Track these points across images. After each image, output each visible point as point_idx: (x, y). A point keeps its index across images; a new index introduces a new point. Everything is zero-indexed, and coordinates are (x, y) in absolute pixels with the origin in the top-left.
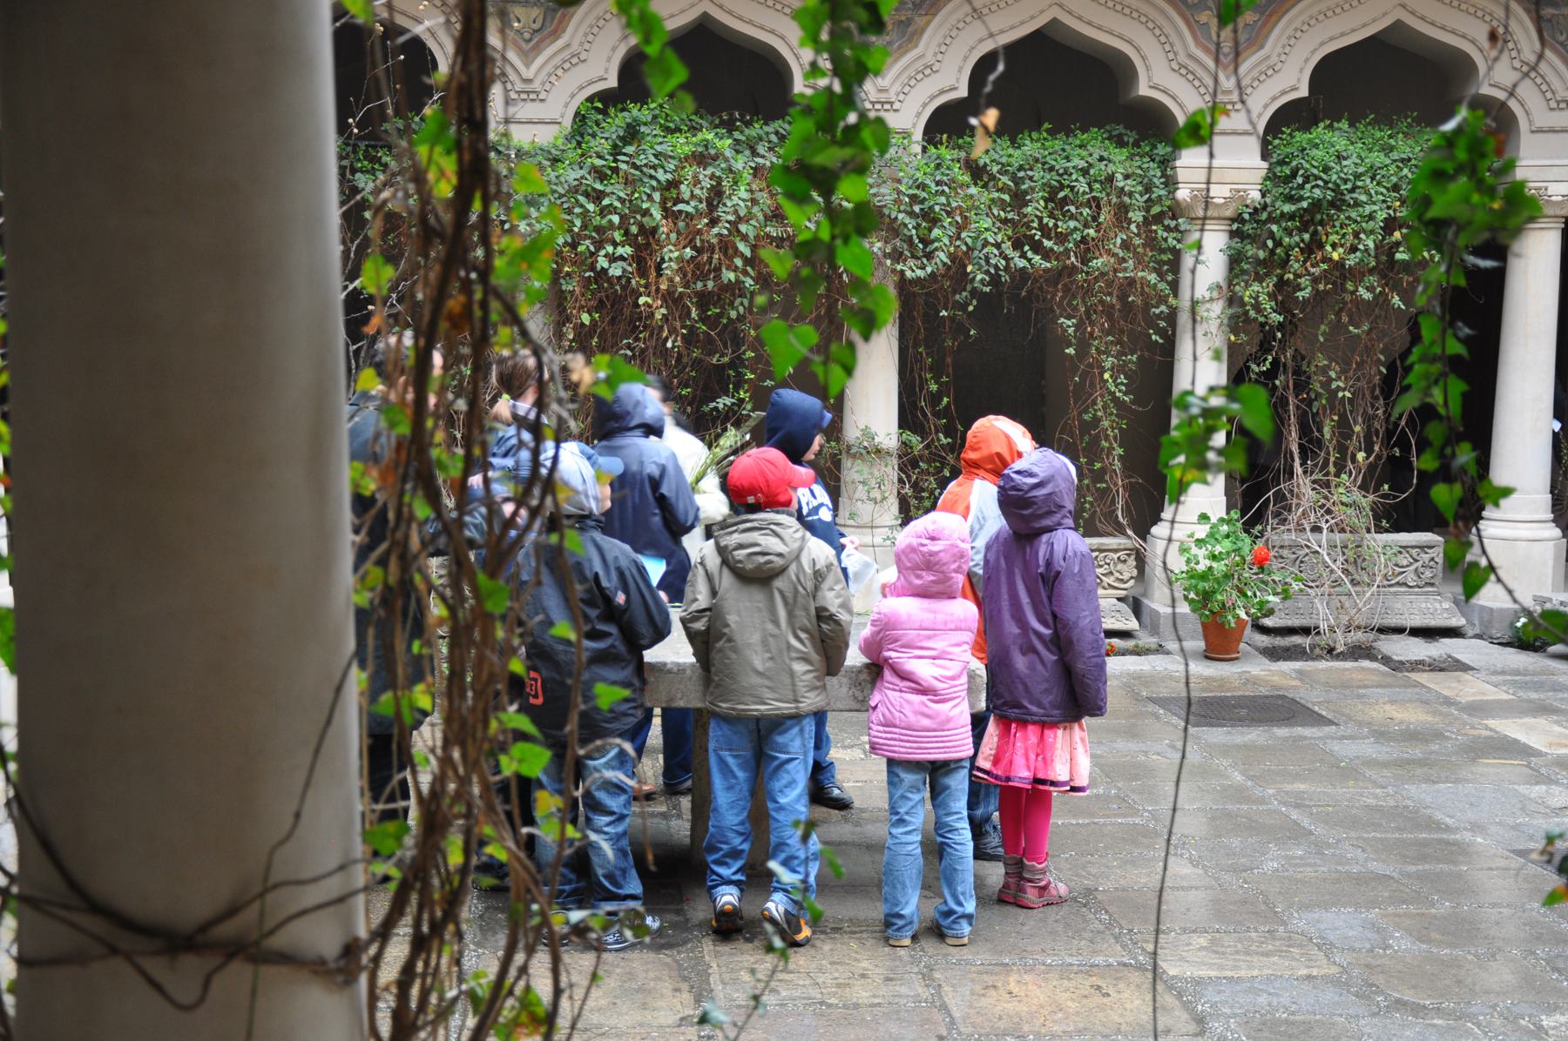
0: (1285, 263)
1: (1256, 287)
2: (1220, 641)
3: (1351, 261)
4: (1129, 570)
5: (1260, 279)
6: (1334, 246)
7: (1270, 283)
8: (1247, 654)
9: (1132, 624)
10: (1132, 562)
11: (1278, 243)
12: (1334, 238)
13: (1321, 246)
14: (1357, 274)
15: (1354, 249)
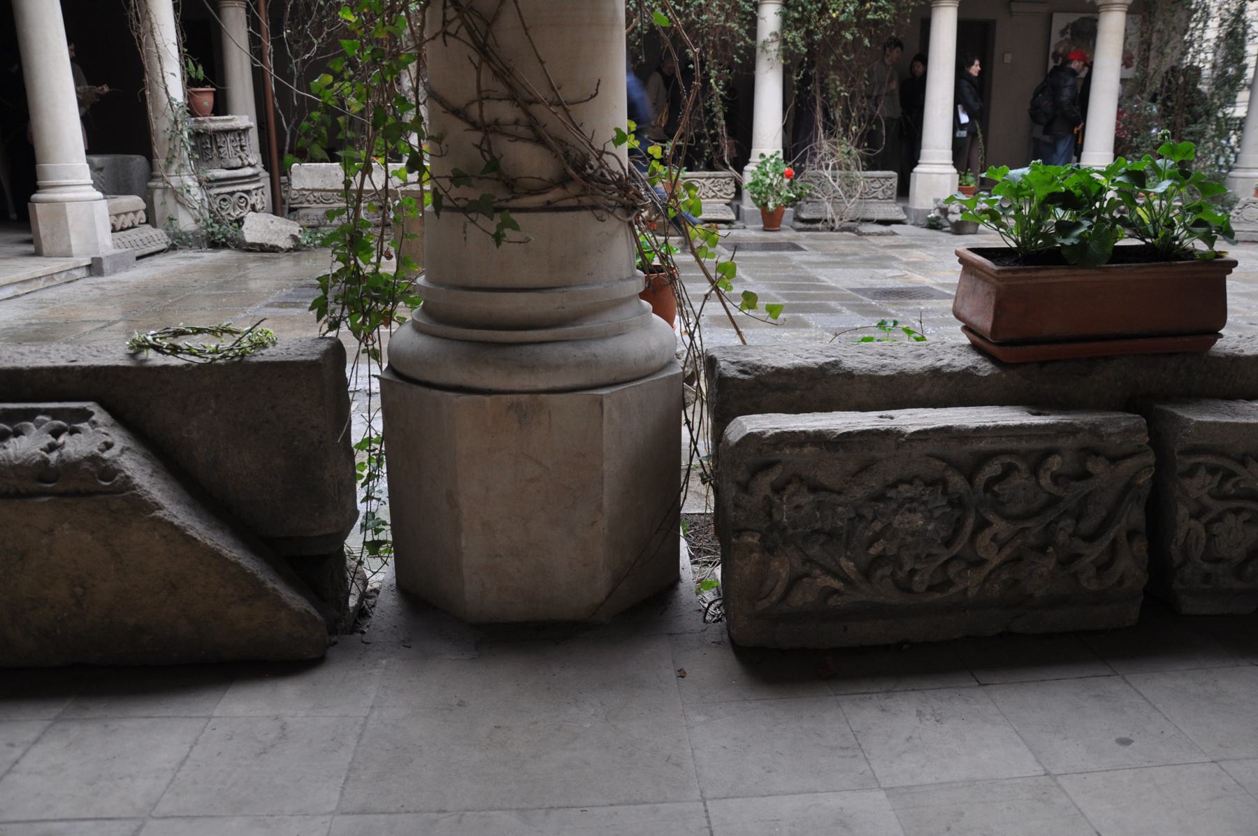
0: (809, 22)
1: (794, 33)
2: (771, 221)
3: (842, 18)
4: (731, 189)
5: (797, 29)
6: (834, 11)
7: (803, 31)
8: (784, 229)
9: (732, 217)
10: (733, 184)
11: (804, 9)
12: (834, 6)
13: (827, 10)
14: (845, 26)
15: (843, 12)
